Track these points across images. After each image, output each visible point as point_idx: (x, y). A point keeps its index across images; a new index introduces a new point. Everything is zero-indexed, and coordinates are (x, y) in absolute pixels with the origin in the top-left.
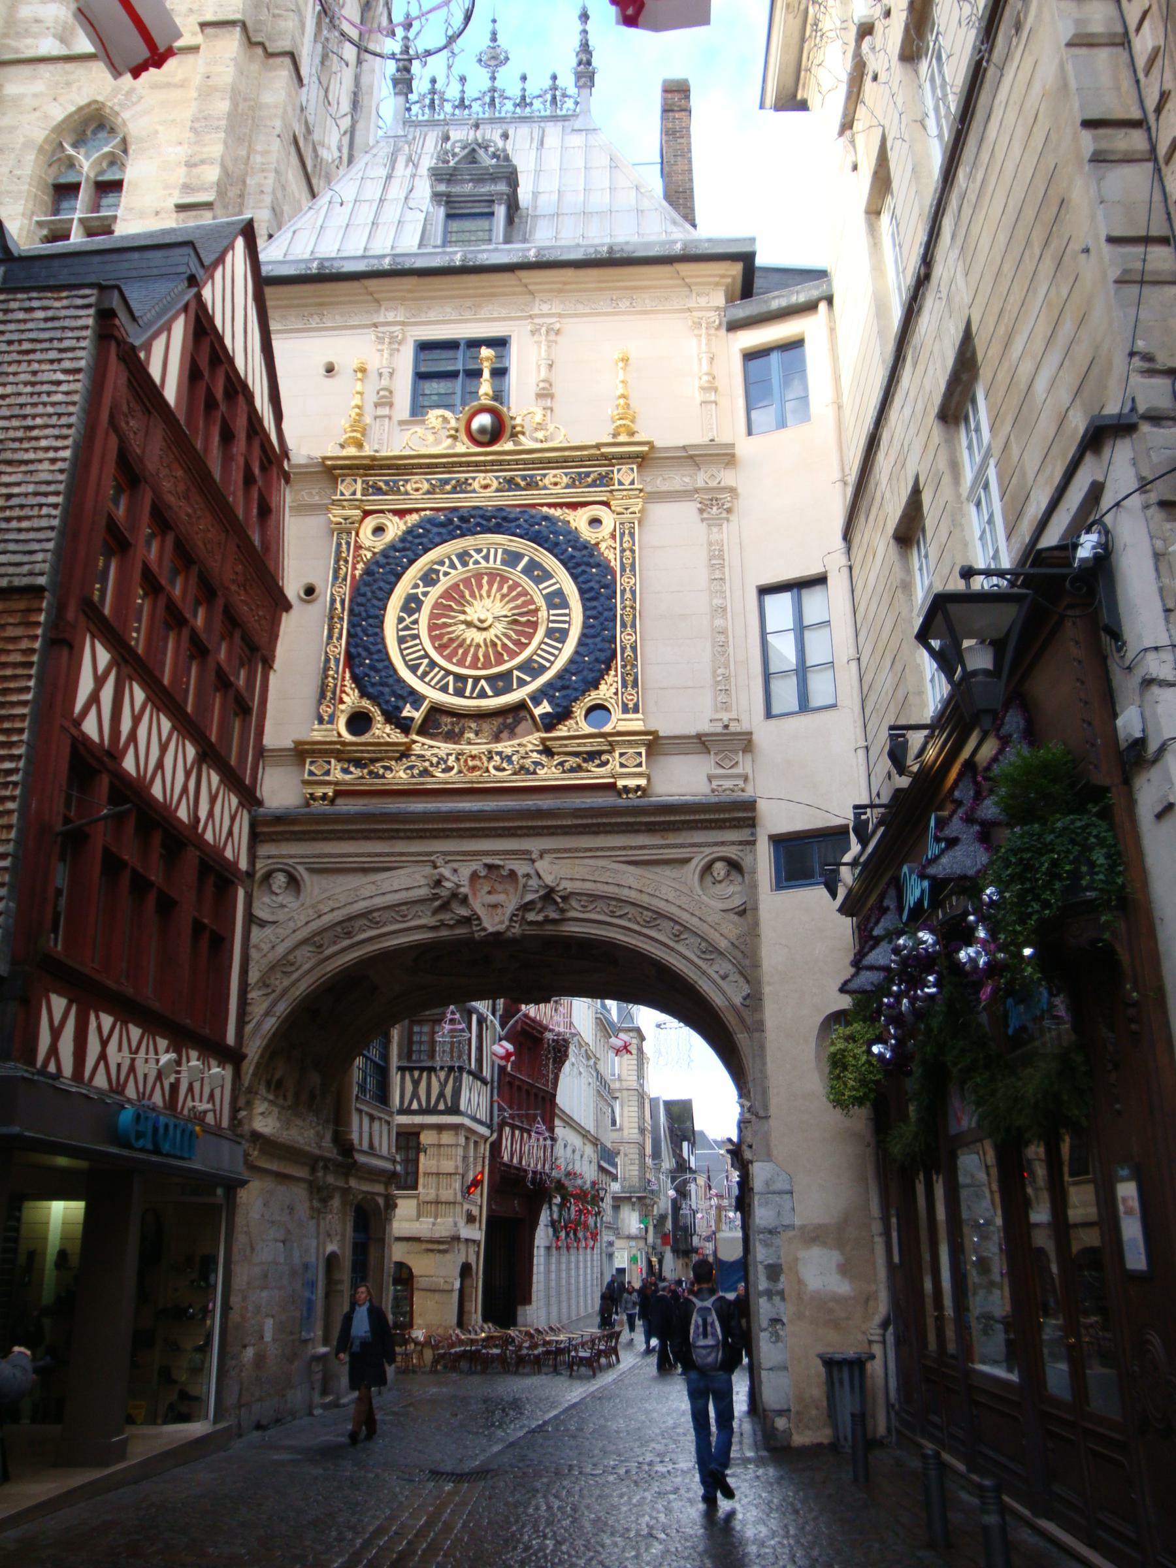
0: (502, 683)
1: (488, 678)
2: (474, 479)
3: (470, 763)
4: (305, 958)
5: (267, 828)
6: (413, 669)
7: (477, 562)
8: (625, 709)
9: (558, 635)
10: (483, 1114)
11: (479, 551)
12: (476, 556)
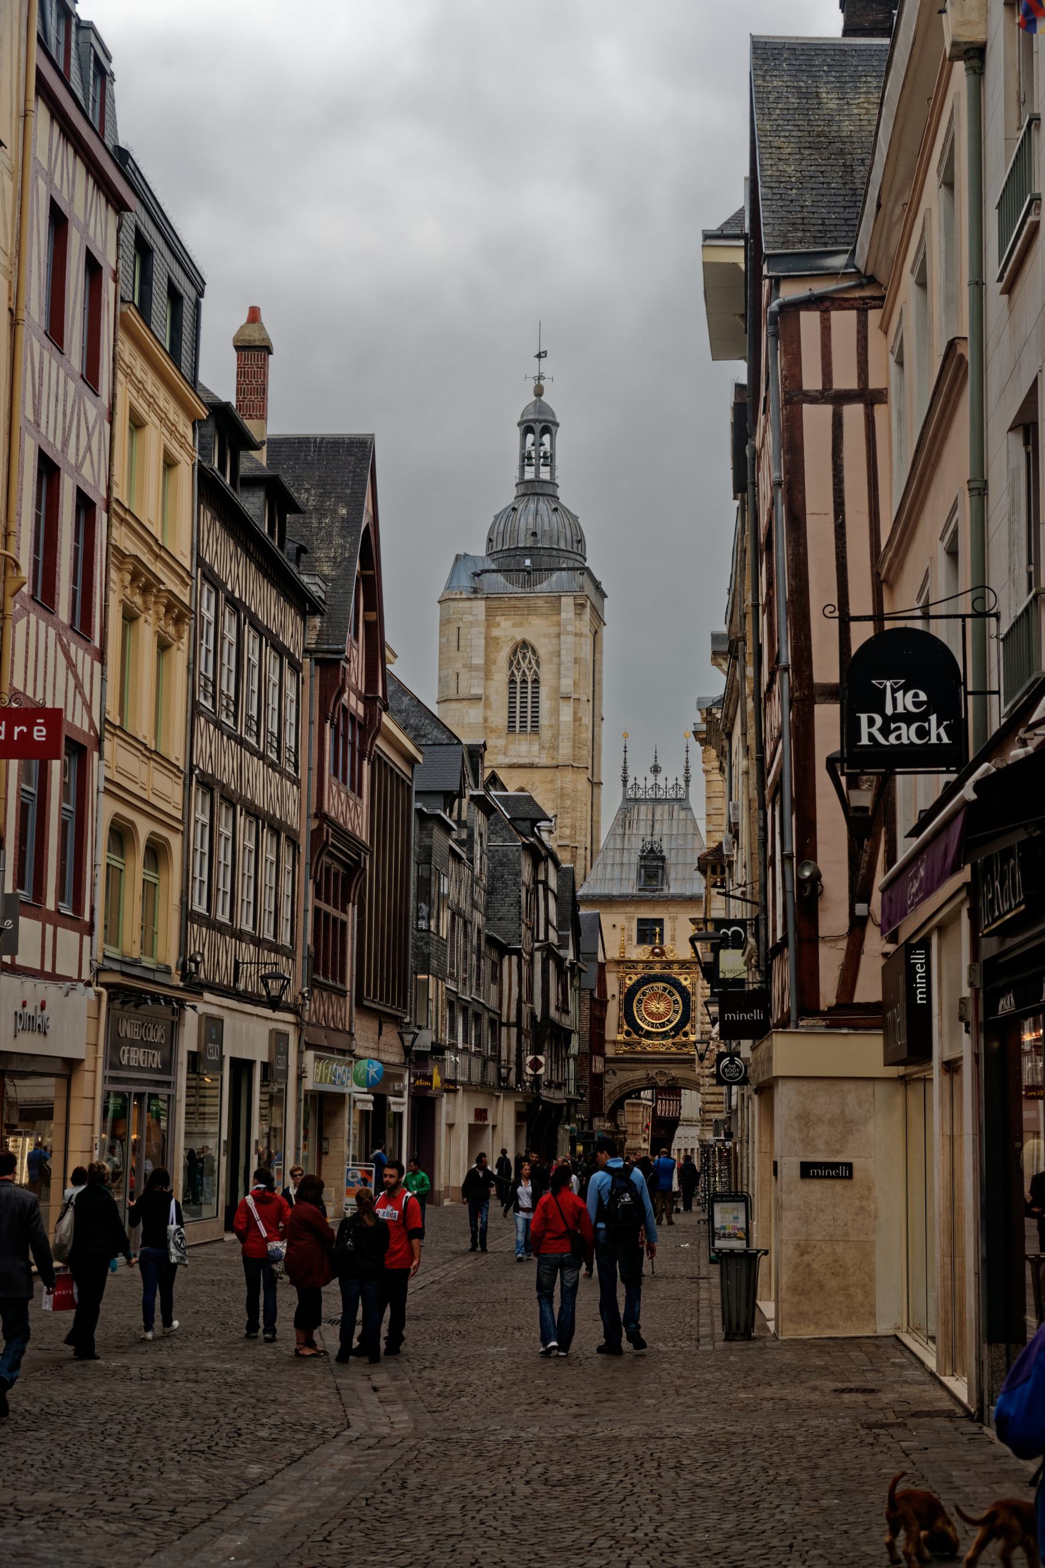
0: (663, 1025)
4: (618, 1091)
5: (608, 1061)
10: (649, 1097)
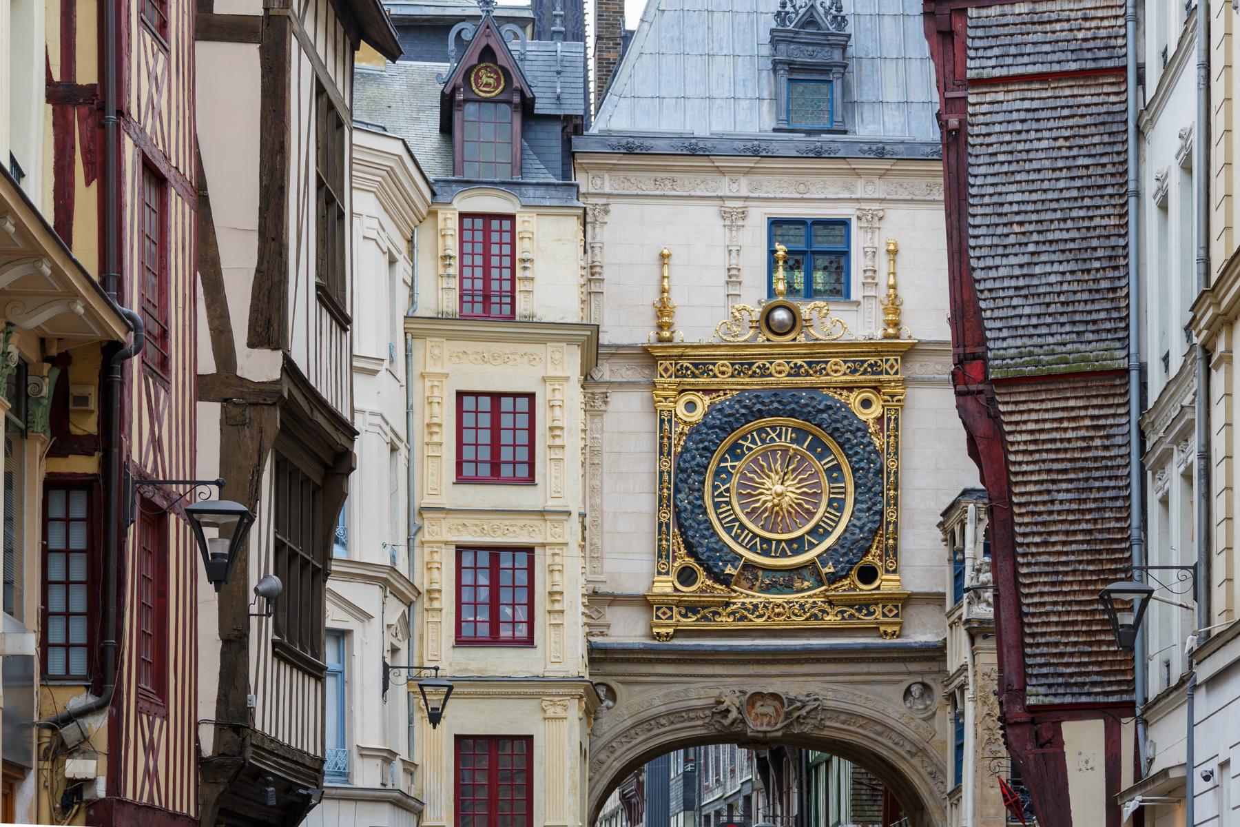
0: (798, 545)
1: (785, 541)
2: (771, 363)
3: (777, 610)
6: (728, 530)
7: (772, 440)
8: (887, 571)
9: (836, 504)
11: (773, 428)
12: (773, 435)
